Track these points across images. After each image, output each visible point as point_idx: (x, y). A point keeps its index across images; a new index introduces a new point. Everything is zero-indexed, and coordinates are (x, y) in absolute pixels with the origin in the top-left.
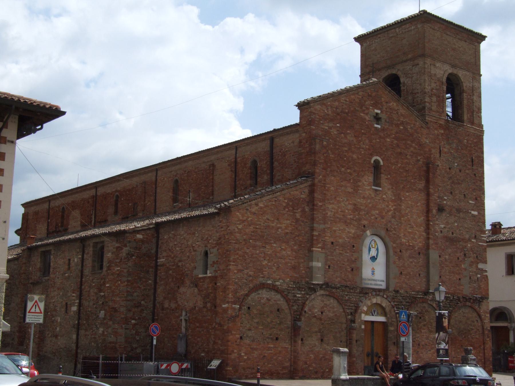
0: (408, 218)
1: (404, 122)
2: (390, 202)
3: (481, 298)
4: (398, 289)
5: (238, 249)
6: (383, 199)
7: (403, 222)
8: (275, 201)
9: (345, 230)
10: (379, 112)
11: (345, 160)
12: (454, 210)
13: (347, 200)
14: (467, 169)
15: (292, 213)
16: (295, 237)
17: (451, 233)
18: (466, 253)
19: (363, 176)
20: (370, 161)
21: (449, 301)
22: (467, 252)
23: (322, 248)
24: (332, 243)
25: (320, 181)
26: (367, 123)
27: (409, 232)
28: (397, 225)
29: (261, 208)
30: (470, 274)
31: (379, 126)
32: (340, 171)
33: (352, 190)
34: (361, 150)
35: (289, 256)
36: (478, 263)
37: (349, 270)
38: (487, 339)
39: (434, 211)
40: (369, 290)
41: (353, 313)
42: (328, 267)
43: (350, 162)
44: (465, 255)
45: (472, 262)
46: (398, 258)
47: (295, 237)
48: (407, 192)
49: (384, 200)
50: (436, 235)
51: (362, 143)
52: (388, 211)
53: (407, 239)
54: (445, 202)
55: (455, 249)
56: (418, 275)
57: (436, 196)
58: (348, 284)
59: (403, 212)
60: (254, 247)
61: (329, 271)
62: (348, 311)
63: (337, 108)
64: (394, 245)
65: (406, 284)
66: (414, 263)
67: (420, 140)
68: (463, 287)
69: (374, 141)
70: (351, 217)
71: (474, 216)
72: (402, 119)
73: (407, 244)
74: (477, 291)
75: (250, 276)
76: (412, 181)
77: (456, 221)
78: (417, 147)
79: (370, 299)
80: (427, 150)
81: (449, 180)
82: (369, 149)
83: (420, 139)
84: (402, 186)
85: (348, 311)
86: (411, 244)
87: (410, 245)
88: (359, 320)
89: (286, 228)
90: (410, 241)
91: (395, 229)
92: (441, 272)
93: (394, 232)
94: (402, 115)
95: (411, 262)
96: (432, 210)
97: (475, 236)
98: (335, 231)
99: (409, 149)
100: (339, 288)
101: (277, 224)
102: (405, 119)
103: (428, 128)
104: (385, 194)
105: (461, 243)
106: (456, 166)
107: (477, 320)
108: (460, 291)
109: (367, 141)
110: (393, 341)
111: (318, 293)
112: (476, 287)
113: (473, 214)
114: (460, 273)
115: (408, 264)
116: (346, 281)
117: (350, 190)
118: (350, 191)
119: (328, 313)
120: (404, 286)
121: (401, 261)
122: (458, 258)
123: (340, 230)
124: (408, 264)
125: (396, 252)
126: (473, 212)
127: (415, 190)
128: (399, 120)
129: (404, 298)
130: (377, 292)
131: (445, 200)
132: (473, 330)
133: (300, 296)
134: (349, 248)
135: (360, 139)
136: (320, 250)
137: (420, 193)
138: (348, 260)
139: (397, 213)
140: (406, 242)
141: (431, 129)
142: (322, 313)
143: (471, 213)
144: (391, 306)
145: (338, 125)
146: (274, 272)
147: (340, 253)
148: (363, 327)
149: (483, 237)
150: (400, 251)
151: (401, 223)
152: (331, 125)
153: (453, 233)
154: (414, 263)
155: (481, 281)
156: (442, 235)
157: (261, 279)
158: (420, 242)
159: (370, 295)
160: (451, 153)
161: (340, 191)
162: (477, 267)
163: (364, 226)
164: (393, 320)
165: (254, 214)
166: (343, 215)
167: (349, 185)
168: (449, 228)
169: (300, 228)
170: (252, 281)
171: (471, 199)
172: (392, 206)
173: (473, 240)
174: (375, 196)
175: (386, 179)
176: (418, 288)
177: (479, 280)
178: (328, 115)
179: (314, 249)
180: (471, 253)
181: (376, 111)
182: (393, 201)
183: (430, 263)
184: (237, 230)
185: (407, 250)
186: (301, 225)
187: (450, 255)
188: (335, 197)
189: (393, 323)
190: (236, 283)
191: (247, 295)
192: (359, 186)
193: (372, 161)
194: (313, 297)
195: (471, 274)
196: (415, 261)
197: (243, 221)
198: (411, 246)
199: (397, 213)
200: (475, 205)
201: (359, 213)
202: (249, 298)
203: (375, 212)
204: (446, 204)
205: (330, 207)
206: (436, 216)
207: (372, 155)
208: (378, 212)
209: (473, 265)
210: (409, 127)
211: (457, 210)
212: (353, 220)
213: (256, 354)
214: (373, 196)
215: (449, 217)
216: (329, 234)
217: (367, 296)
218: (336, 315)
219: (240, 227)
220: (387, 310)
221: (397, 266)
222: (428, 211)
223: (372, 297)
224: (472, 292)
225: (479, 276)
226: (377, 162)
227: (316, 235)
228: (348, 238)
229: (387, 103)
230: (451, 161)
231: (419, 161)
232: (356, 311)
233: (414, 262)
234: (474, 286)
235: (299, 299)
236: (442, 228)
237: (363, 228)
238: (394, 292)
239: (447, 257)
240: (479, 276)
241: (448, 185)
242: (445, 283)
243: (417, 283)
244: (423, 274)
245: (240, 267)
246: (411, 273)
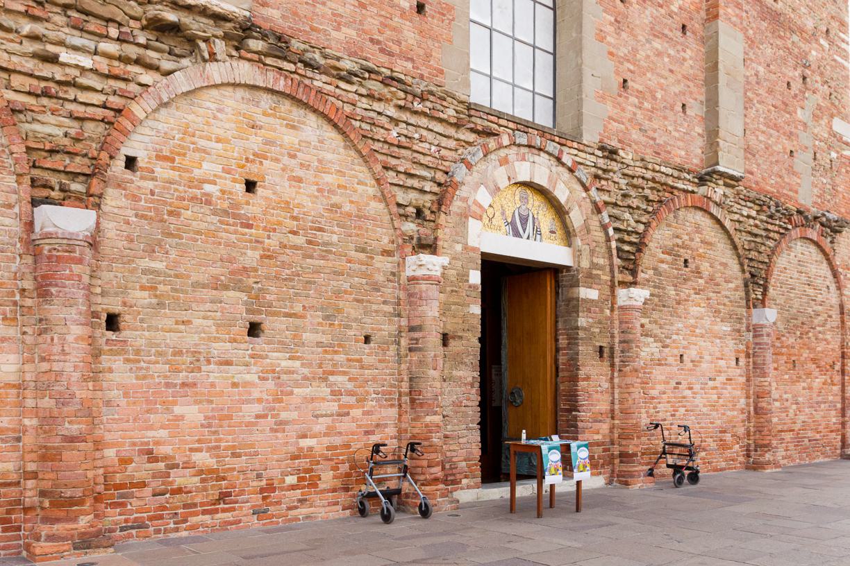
4: (614, 143)
21: (765, 218)
40: (502, 122)
41: (427, 212)
58: (402, 68)
62: (401, 197)
66: (666, 60)
68: (799, 181)
74: (829, 201)
79: (504, 161)
85: (401, 197)
88: (459, 247)
95: (659, 54)
100: (348, 77)
108: (790, 190)
110: (598, 344)
111: (216, 72)
115: (648, 57)
119: (287, 190)
129: (635, 181)
133: (87, 62)
142: (250, 186)
144: (590, 206)
148: (475, 277)
164: (595, 260)
176: (679, 156)
183: (721, 66)
187: (768, 66)
189: (595, 272)
194: (181, 82)
196: (672, 52)
218: (335, 207)
220: (576, 218)
225: (834, 155)
232: (441, 202)
233: (669, 56)
235: (83, 81)
238: (599, 153)
243: (677, 135)
244: (696, 110)
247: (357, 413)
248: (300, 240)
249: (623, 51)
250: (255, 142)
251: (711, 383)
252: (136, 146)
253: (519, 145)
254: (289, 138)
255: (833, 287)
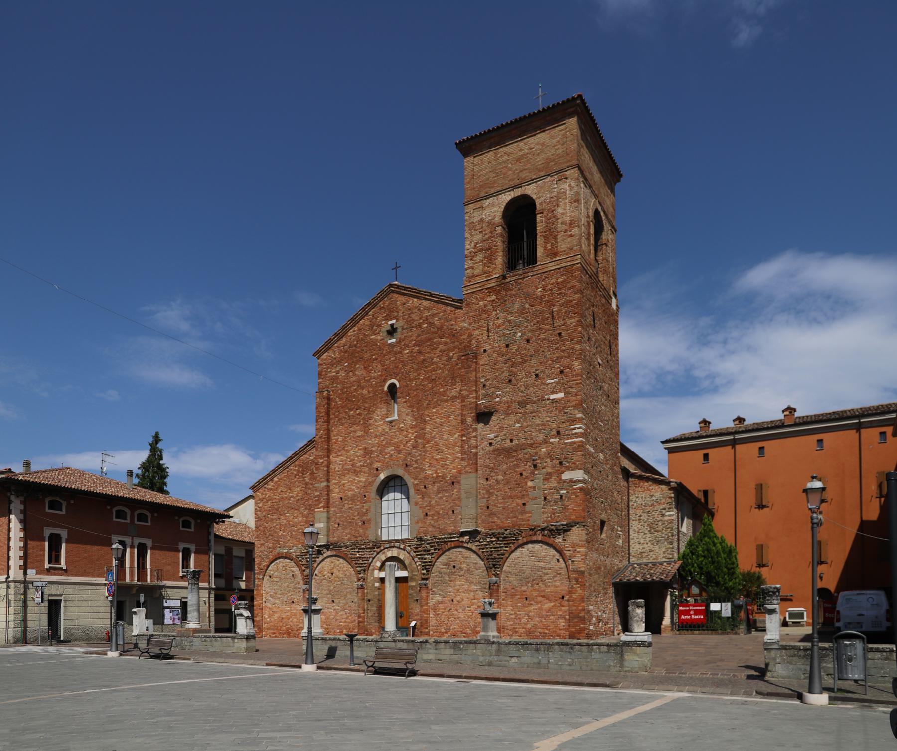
0: (435, 442)
1: (429, 316)
2: (410, 431)
3: (566, 525)
5: (260, 526)
6: (400, 430)
7: (428, 449)
8: (287, 471)
9: (355, 480)
10: (394, 322)
11: (353, 401)
12: (516, 405)
13: (357, 446)
14: (542, 332)
15: (301, 480)
16: (305, 503)
17: (508, 441)
18: (538, 463)
19: (374, 411)
20: (383, 389)
22: (538, 461)
23: (324, 507)
24: (341, 498)
25: (321, 437)
26: (379, 344)
27: (436, 460)
28: (420, 455)
29: (276, 482)
30: (545, 494)
31: (394, 340)
32: (349, 416)
33: (363, 432)
34: (371, 380)
35: (301, 522)
36: (563, 472)
37: (360, 524)
38: (574, 586)
39: (469, 420)
42: (337, 526)
43: (359, 400)
44: (535, 466)
45: (550, 474)
46: (421, 496)
47: (305, 503)
48: (434, 408)
49: (402, 430)
50: (471, 452)
51: (373, 372)
52: (407, 442)
53: (435, 469)
54: (498, 399)
55: (515, 463)
56: (451, 512)
57: (473, 397)
59: (428, 436)
60: (272, 520)
61: (338, 530)
63: (343, 347)
64: (416, 482)
65: (434, 527)
66: (444, 498)
67: (452, 329)
68: (530, 515)
69: (387, 362)
70: (362, 463)
71: (554, 401)
72: (426, 314)
73: (434, 475)
74: (558, 516)
75: (270, 548)
76: (441, 390)
77: (518, 421)
78: (448, 340)
80: (465, 337)
81: (505, 364)
82: (381, 376)
83: (452, 327)
84: (425, 404)
86: (440, 475)
87: (438, 477)
89: (297, 496)
90: (438, 471)
91: (416, 462)
92: (488, 501)
93: (415, 466)
94: (426, 309)
95: (441, 498)
96: (466, 419)
97: (558, 432)
98: (344, 485)
99: (436, 349)
101: (289, 493)
102: (431, 312)
103: (468, 305)
104: (403, 422)
105: (526, 451)
106: (520, 337)
107: (558, 560)
109: (379, 367)
111: (325, 555)
112: (558, 509)
113: (553, 399)
114: (524, 495)
115: (436, 501)
116: (356, 537)
117: (360, 433)
118: (360, 434)
120: (430, 530)
121: (425, 499)
122: (521, 475)
123: (348, 483)
124: (436, 501)
125: (418, 490)
126: (552, 397)
127: (446, 401)
128: (421, 318)
130: (391, 544)
131: (498, 396)
132: (547, 574)
134: (359, 499)
135: (370, 368)
136: (322, 509)
137: (453, 402)
138: (358, 513)
139: (419, 441)
140: (432, 474)
141: (474, 303)
143: (549, 399)
145: (346, 364)
146: (288, 540)
147: (350, 508)
149: (574, 429)
150: (425, 487)
151: (425, 451)
152: (338, 369)
153: (511, 440)
154: (444, 498)
155: (569, 499)
156: (491, 448)
157: (278, 549)
158: (454, 468)
159: (382, 548)
160: (509, 322)
161: (348, 438)
162: (561, 479)
163: (377, 470)
165: (271, 490)
166: (352, 465)
167: (359, 427)
168: (505, 435)
169: (309, 492)
170: (271, 552)
171: (549, 377)
172: (412, 434)
173: (552, 440)
174: (390, 429)
175: (404, 402)
177: (563, 497)
178: (335, 359)
179: (316, 510)
180: (548, 460)
181: (390, 323)
182: (412, 427)
184: (258, 509)
185: (434, 483)
186: (310, 489)
187: (505, 473)
188: (344, 447)
190: (260, 556)
191: (268, 566)
192: (370, 424)
193: (386, 388)
195: (546, 492)
197: (262, 499)
198: (440, 476)
199: (419, 441)
200: (557, 383)
201: (370, 457)
202: (270, 568)
203: (389, 449)
204: (499, 402)
205: (338, 460)
206: (472, 425)
207: (385, 381)
208: (393, 447)
209: (551, 478)
210: (436, 319)
211: (520, 403)
212: (364, 466)
213: (276, 616)
214: (387, 430)
215: (503, 418)
216: (337, 491)
217: (378, 550)
219: (260, 505)
221: (420, 507)
222: (463, 421)
223: (386, 550)
224: (549, 519)
226: (392, 386)
227: (318, 495)
228: (358, 489)
229: (404, 304)
230: (510, 334)
231: (451, 358)
234: (553, 509)
236: (493, 439)
237: (375, 472)
239: (500, 477)
240: (562, 492)
241: (503, 372)
242: (495, 515)
245: (262, 541)
246: (441, 512)
247: (350, 618)
248: (340, 583)
249: (425, 504)
250: (332, 565)
251: (468, 609)
252: (316, 572)
253: (387, 548)
254: (338, 563)
255: (561, 560)
